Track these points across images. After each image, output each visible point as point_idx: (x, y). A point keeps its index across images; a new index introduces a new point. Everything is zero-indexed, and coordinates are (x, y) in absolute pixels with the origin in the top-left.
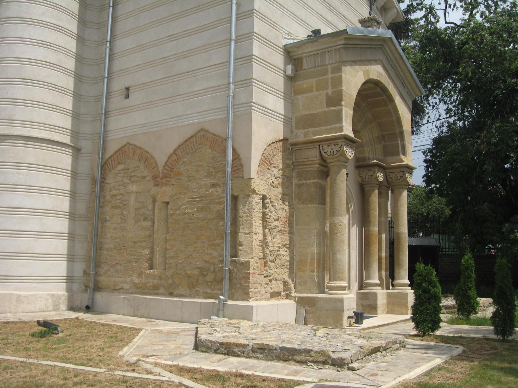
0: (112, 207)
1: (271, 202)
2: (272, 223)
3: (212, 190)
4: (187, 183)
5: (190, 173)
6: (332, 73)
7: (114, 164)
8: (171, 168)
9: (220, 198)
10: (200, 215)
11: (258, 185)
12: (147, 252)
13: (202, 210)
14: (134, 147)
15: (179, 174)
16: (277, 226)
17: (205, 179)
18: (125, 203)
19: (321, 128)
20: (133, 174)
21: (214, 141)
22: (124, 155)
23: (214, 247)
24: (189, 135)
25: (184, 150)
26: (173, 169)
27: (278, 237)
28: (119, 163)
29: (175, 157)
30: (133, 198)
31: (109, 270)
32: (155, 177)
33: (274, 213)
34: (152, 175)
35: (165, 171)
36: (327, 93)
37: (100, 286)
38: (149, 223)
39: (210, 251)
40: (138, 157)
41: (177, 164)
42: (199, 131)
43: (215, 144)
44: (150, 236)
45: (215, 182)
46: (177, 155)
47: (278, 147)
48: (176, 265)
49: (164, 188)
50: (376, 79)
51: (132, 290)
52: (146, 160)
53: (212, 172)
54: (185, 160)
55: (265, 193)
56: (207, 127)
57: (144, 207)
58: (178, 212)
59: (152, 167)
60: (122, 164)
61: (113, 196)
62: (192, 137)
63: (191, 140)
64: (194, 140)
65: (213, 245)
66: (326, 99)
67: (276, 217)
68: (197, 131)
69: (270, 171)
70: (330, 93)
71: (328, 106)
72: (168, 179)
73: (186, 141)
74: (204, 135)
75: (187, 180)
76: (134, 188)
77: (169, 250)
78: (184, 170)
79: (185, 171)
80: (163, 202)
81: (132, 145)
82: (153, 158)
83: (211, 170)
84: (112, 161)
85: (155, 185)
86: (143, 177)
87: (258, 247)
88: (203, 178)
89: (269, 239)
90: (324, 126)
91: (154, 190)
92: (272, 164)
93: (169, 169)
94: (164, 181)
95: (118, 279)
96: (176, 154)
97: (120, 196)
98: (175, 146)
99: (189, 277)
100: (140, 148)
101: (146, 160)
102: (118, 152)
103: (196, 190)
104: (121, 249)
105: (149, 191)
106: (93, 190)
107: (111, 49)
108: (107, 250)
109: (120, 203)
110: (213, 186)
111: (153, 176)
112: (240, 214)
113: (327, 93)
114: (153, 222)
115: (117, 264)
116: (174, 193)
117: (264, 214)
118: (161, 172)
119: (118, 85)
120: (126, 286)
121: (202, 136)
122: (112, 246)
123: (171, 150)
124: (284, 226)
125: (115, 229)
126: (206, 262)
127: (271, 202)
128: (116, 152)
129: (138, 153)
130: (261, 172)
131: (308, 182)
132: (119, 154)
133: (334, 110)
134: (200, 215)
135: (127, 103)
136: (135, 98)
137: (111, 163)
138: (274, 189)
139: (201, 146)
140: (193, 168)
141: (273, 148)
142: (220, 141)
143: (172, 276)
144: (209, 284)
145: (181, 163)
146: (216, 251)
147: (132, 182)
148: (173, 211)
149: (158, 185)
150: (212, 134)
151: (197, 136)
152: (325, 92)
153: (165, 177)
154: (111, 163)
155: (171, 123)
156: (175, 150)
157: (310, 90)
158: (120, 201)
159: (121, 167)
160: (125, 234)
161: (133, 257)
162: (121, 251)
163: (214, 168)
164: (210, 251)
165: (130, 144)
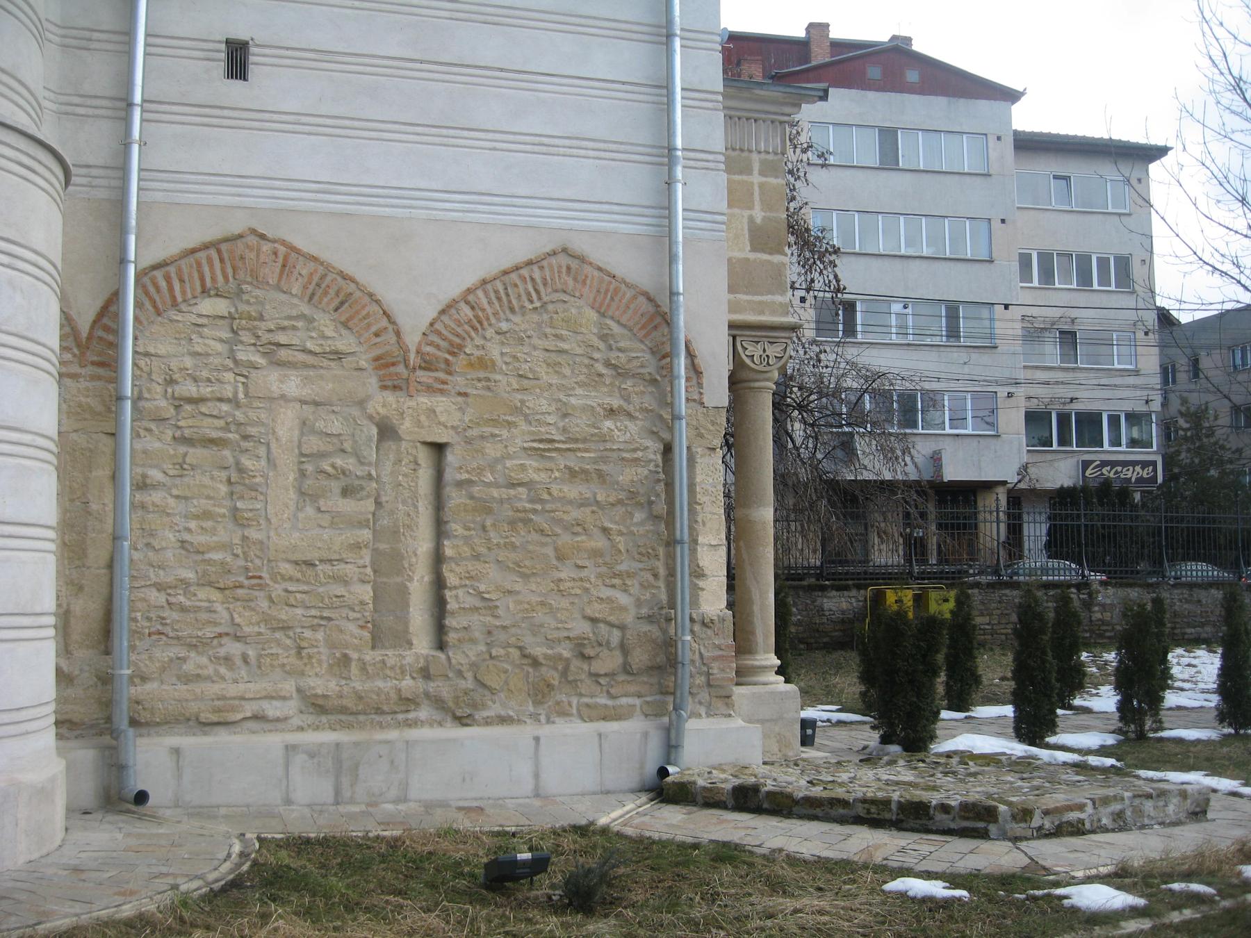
3: (609, 424)
4: (519, 396)
5: (526, 366)
7: (184, 292)
8: (451, 344)
9: (635, 450)
14: (282, 250)
15: (483, 363)
17: (579, 391)
18: (252, 430)
19: (738, 296)
20: (282, 338)
21: (607, 290)
22: (234, 269)
23: (617, 581)
24: (522, 256)
25: (499, 299)
26: (460, 347)
28: (205, 291)
29: (466, 311)
31: (184, 660)
32: (382, 363)
34: (378, 352)
35: (428, 349)
36: (751, 220)
37: (144, 717)
39: (606, 593)
40: (305, 288)
41: (473, 334)
42: (555, 253)
43: (612, 299)
45: (616, 402)
46: (473, 308)
48: (489, 633)
49: (424, 400)
51: (296, 721)
52: (342, 303)
53: (600, 375)
54: (504, 326)
56: (581, 245)
57: (343, 451)
58: (489, 478)
59: (374, 329)
60: (217, 295)
61: (179, 402)
62: (530, 263)
63: (524, 272)
65: (615, 575)
66: (750, 230)
68: (548, 249)
70: (759, 220)
71: (754, 249)
72: (441, 375)
74: (569, 268)
75: (516, 386)
76: (293, 385)
77: (455, 588)
78: (502, 354)
79: (507, 359)
80: (425, 443)
81: (274, 241)
82: (378, 302)
83: (600, 368)
84: (168, 278)
85: (384, 388)
86: (338, 356)
88: (573, 389)
90: (747, 294)
93: (443, 344)
94: (423, 376)
95: (233, 690)
96: (467, 303)
97: (225, 407)
98: (471, 279)
100: (314, 259)
101: (342, 303)
102: (202, 255)
103: (550, 419)
104: (241, 587)
105: (361, 404)
106: (64, 370)
108: (160, 587)
109: (226, 429)
110: (611, 413)
111: (377, 359)
112: (698, 496)
113: (751, 220)
115: (220, 635)
116: (467, 420)
118: (413, 349)
121: (564, 270)
122: (190, 575)
123: (454, 289)
126: (594, 620)
129: (304, 272)
132: (204, 262)
133: (769, 261)
134: (572, 491)
137: (163, 284)
139: (566, 298)
140: (535, 353)
142: (628, 295)
143: (474, 666)
144: (602, 681)
145: (490, 332)
146: (625, 591)
148: (468, 472)
149: (396, 388)
150: (600, 269)
151: (545, 263)
152: (746, 213)
153: (428, 365)
154: (163, 284)
155: (447, 206)
156: (469, 291)
158: (221, 423)
159: (209, 306)
160: (253, 534)
161: (299, 611)
162: (240, 592)
163: (608, 364)
164: (606, 593)
165: (263, 237)
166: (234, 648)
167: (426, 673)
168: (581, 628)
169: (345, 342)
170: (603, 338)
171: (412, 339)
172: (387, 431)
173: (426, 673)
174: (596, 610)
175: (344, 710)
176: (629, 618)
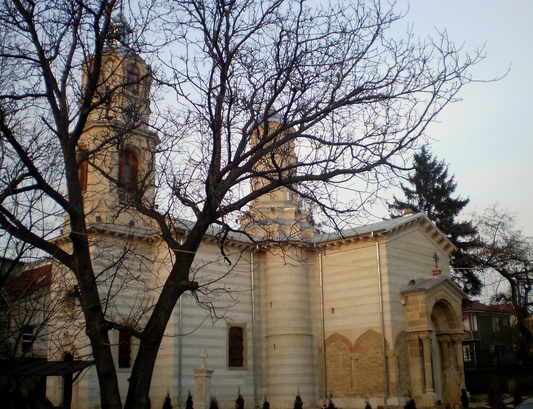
0: (331, 361)
3: (377, 355)
6: (421, 304)
10: (373, 365)
12: (350, 380)
13: (373, 362)
15: (362, 348)
30: (341, 358)
32: (350, 349)
38: (349, 368)
39: (379, 379)
44: (350, 374)
45: (378, 351)
49: (356, 354)
62: (366, 333)
64: (367, 334)
73: (364, 334)
76: (341, 353)
83: (376, 347)
86: (345, 349)
91: (351, 354)
99: (370, 389)
107: (322, 290)
110: (378, 353)
114: (351, 367)
117: (398, 363)
119: (328, 307)
120: (341, 395)
122: (332, 378)
125: (333, 371)
128: (330, 337)
131: (415, 348)
134: (373, 365)
135: (333, 315)
136: (337, 313)
147: (340, 350)
157: (412, 310)
159: (333, 344)
166: (337, 388)
167: (357, 391)
168: (375, 384)
169: (346, 347)
170: (376, 342)
171: (353, 345)
172: (351, 358)
173: (357, 391)
174: (377, 382)
175: (348, 396)
176: (381, 383)
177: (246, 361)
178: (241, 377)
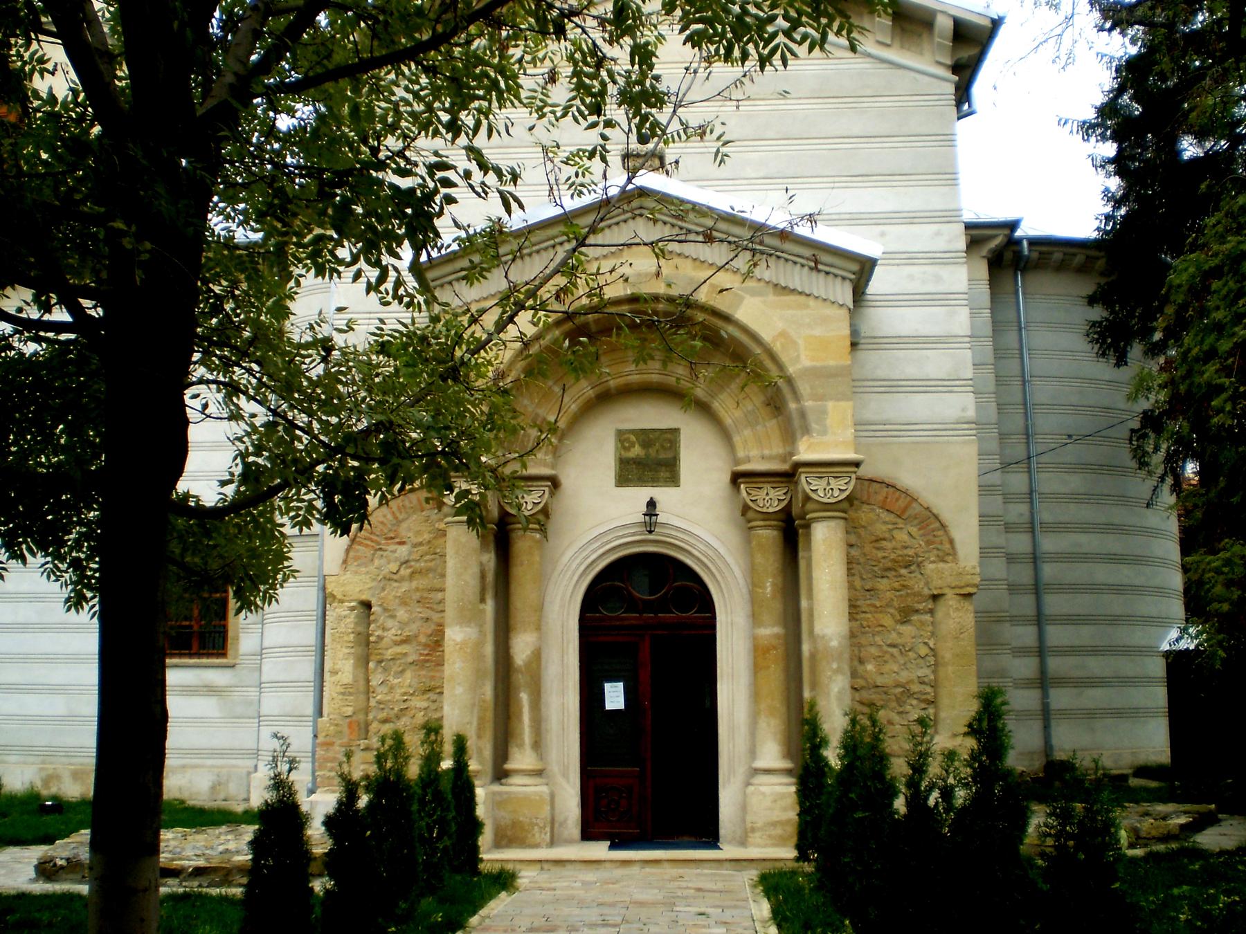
1: (386, 610)
2: (387, 649)
11: (343, 585)
16: (405, 654)
27: (408, 674)
33: (393, 631)
47: (411, 502)
50: (622, 294)
55: (364, 597)
67: (398, 638)
69: (385, 554)
87: (341, 697)
89: (375, 680)
92: (392, 538)
124: (426, 652)
127: (386, 610)
130: (356, 558)
138: (396, 584)
141: (395, 509)
177: (237, 638)
178: (210, 690)
